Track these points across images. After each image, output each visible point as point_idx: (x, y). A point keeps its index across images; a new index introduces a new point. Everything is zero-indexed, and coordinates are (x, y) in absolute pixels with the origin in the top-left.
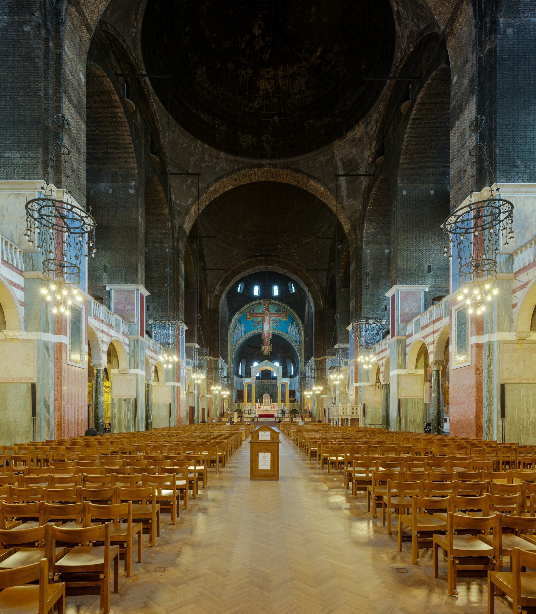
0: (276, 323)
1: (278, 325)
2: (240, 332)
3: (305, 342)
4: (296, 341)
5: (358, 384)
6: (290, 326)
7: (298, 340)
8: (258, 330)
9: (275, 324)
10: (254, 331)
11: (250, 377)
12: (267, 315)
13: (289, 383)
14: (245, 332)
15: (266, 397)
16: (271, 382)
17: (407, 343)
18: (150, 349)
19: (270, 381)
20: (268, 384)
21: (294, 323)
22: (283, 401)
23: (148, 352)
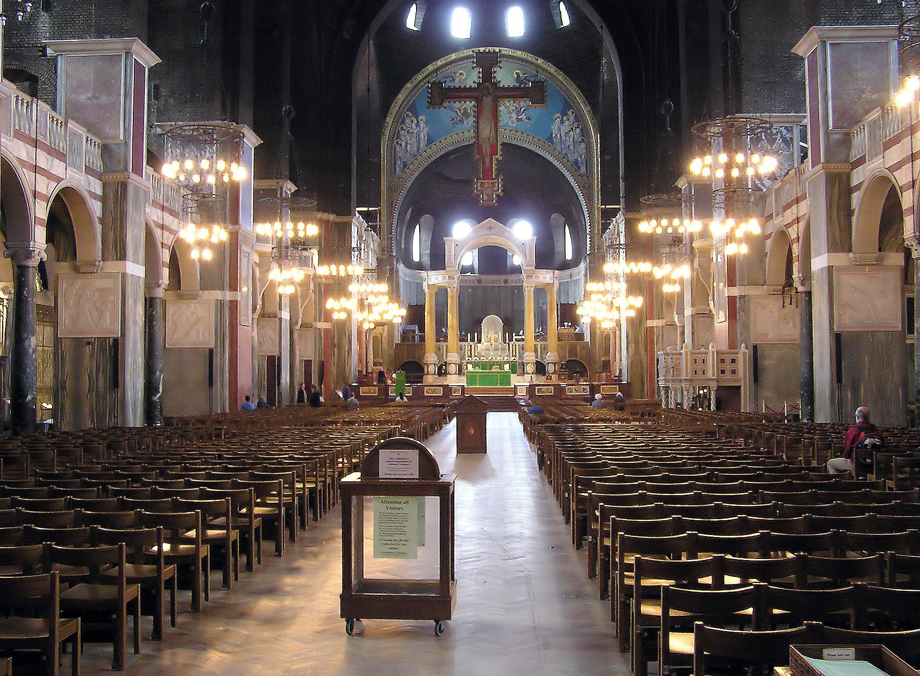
1: (523, 116)
4: (576, 162)
5: (735, 291)
9: (514, 115)
13: (556, 285)
14: (430, 141)
15: (492, 327)
16: (506, 282)
17: (855, 182)
18: (159, 204)
19: (503, 277)
21: (570, 113)
22: (541, 336)
23: (154, 215)
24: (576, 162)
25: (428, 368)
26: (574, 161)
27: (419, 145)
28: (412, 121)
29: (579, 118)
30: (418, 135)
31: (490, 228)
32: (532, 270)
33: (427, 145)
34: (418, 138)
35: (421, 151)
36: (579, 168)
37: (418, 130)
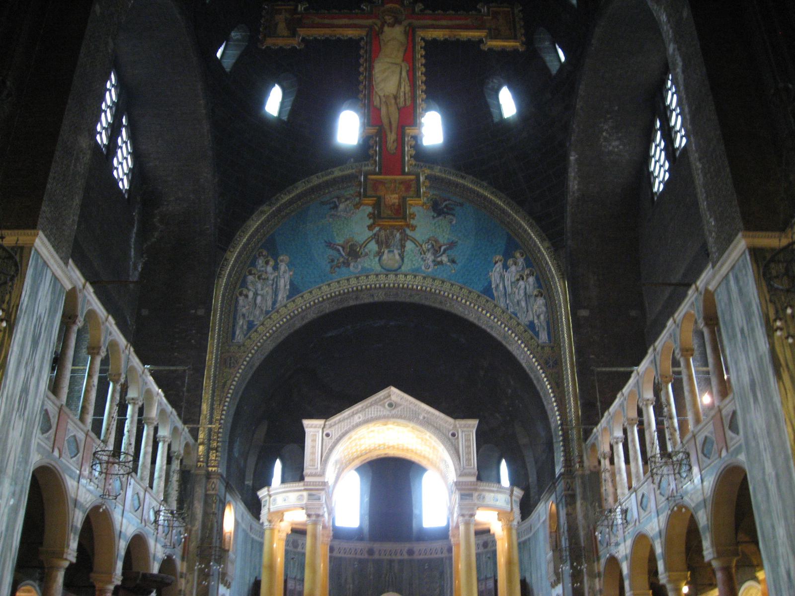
0: (436, 251)
1: (444, 259)
2: (268, 290)
3: (578, 325)
4: (531, 325)
6: (500, 264)
7: (540, 322)
8: (353, 282)
9: (430, 257)
10: (334, 285)
11: (302, 478)
12: (397, 22)
14: (294, 290)
19: (407, 546)
20: (401, 561)
24: (531, 325)
26: (528, 323)
27: (276, 295)
28: (267, 263)
29: (533, 264)
30: (276, 282)
31: (390, 405)
32: (471, 483)
33: (289, 297)
34: (274, 286)
35: (278, 305)
36: (537, 334)
37: (276, 274)
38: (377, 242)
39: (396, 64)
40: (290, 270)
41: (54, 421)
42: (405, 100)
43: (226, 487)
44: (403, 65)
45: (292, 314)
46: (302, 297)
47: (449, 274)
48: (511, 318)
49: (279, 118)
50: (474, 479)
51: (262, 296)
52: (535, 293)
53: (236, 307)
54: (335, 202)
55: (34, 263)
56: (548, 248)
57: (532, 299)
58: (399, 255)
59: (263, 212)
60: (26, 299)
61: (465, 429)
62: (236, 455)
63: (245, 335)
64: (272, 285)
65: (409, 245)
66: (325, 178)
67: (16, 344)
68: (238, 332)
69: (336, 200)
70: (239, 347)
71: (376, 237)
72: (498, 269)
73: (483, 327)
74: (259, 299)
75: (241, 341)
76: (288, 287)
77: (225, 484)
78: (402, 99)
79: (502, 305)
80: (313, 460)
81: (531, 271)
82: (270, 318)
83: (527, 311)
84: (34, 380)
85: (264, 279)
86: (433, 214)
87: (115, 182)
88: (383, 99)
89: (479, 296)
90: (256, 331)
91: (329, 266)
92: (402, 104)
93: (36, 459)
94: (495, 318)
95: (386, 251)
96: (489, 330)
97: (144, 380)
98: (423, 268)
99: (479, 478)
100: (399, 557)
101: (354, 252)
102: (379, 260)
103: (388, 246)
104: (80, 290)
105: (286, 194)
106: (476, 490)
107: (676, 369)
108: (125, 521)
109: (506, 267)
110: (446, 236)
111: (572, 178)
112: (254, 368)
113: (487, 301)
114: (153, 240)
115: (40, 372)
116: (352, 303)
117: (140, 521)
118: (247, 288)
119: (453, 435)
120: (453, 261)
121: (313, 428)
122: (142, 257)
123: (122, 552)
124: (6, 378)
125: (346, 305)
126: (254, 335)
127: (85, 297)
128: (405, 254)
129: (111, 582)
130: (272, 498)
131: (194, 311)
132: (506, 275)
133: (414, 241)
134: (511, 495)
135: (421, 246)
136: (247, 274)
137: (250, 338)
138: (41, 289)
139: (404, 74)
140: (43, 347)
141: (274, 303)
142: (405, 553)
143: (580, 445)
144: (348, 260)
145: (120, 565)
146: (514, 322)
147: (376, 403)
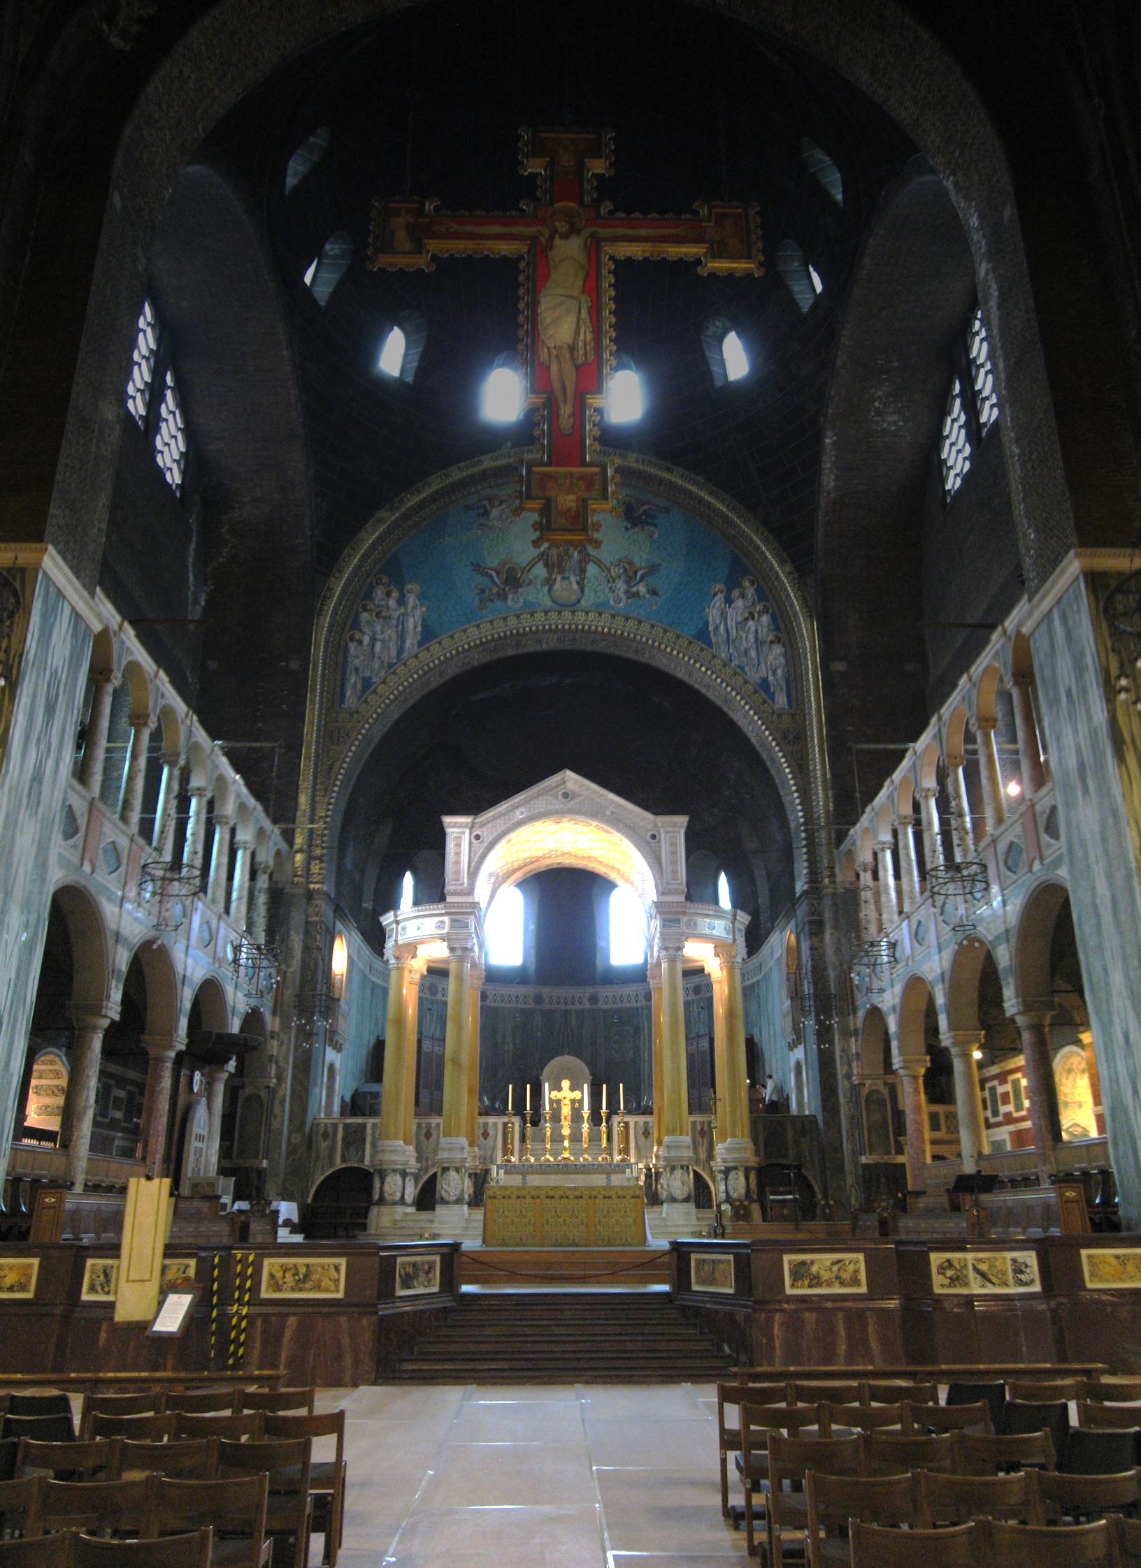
0: (630, 579)
1: (642, 589)
2: (391, 633)
3: (830, 684)
4: (764, 684)
6: (720, 597)
7: (777, 679)
8: (512, 621)
9: (621, 586)
10: (485, 627)
11: (442, 898)
14: (428, 634)
19: (589, 991)
24: (764, 684)
25: (382, 1183)
26: (759, 681)
27: (403, 641)
28: (389, 594)
29: (768, 596)
30: (401, 621)
31: (566, 795)
33: (420, 644)
34: (400, 628)
35: (405, 655)
38: (546, 565)
39: (571, 297)
40: (422, 604)
41: (82, 822)
42: (586, 354)
43: (335, 911)
44: (583, 298)
45: (426, 668)
46: (440, 643)
47: (649, 610)
48: (735, 674)
49: (400, 380)
50: (682, 898)
51: (383, 641)
52: (770, 638)
53: (345, 658)
54: (485, 506)
55: (42, 592)
56: (790, 573)
57: (766, 648)
58: (578, 583)
59: (381, 521)
60: (34, 646)
61: (669, 829)
62: (349, 866)
63: (359, 698)
64: (397, 626)
65: (592, 569)
66: (471, 471)
67: (21, 711)
68: (348, 694)
69: (486, 503)
70: (351, 714)
71: (544, 557)
72: (718, 604)
73: (696, 686)
74: (378, 645)
75: (353, 706)
76: (419, 629)
77: (333, 907)
78: (581, 352)
79: (723, 655)
80: (457, 872)
81: (764, 606)
82: (394, 673)
83: (759, 664)
84: (50, 764)
85: (385, 618)
86: (625, 523)
87: (160, 473)
88: (554, 352)
89: (690, 643)
90: (375, 692)
91: (477, 598)
92: (581, 360)
93: (57, 877)
94: (712, 673)
95: (559, 578)
96: (703, 691)
97: (213, 761)
98: (612, 602)
99: (689, 898)
100: (577, 1007)
101: (513, 579)
102: (549, 590)
103: (561, 571)
104: (115, 632)
105: (413, 494)
106: (684, 913)
107: (970, 747)
108: (190, 961)
109: (729, 601)
110: (645, 557)
111: (826, 471)
112: (373, 745)
113: (702, 650)
114: (222, 560)
115: (60, 751)
116: (510, 652)
117: (211, 961)
118: (361, 630)
119: (653, 837)
120: (654, 593)
121: (458, 829)
122: (206, 584)
123: (187, 1005)
124: (9, 761)
125: (502, 654)
126: (372, 698)
127: (123, 642)
128: (586, 581)
129: (171, 1047)
130: (400, 926)
131: (283, 664)
132: (730, 612)
133: (599, 563)
134: (733, 923)
135: (609, 570)
136: (360, 610)
137: (366, 702)
138: (56, 631)
139: (584, 313)
140: (62, 715)
141: (400, 651)
142: (585, 1000)
143: (831, 853)
144: (504, 590)
145: (183, 1023)
146: (740, 680)
147: (544, 792)
